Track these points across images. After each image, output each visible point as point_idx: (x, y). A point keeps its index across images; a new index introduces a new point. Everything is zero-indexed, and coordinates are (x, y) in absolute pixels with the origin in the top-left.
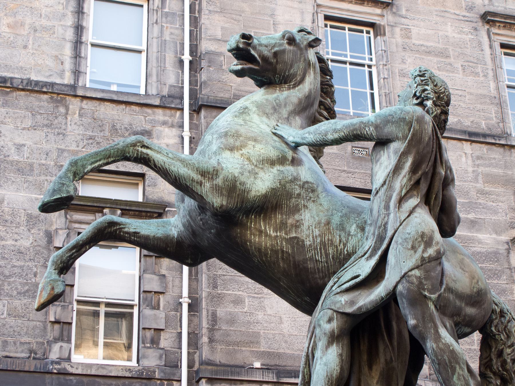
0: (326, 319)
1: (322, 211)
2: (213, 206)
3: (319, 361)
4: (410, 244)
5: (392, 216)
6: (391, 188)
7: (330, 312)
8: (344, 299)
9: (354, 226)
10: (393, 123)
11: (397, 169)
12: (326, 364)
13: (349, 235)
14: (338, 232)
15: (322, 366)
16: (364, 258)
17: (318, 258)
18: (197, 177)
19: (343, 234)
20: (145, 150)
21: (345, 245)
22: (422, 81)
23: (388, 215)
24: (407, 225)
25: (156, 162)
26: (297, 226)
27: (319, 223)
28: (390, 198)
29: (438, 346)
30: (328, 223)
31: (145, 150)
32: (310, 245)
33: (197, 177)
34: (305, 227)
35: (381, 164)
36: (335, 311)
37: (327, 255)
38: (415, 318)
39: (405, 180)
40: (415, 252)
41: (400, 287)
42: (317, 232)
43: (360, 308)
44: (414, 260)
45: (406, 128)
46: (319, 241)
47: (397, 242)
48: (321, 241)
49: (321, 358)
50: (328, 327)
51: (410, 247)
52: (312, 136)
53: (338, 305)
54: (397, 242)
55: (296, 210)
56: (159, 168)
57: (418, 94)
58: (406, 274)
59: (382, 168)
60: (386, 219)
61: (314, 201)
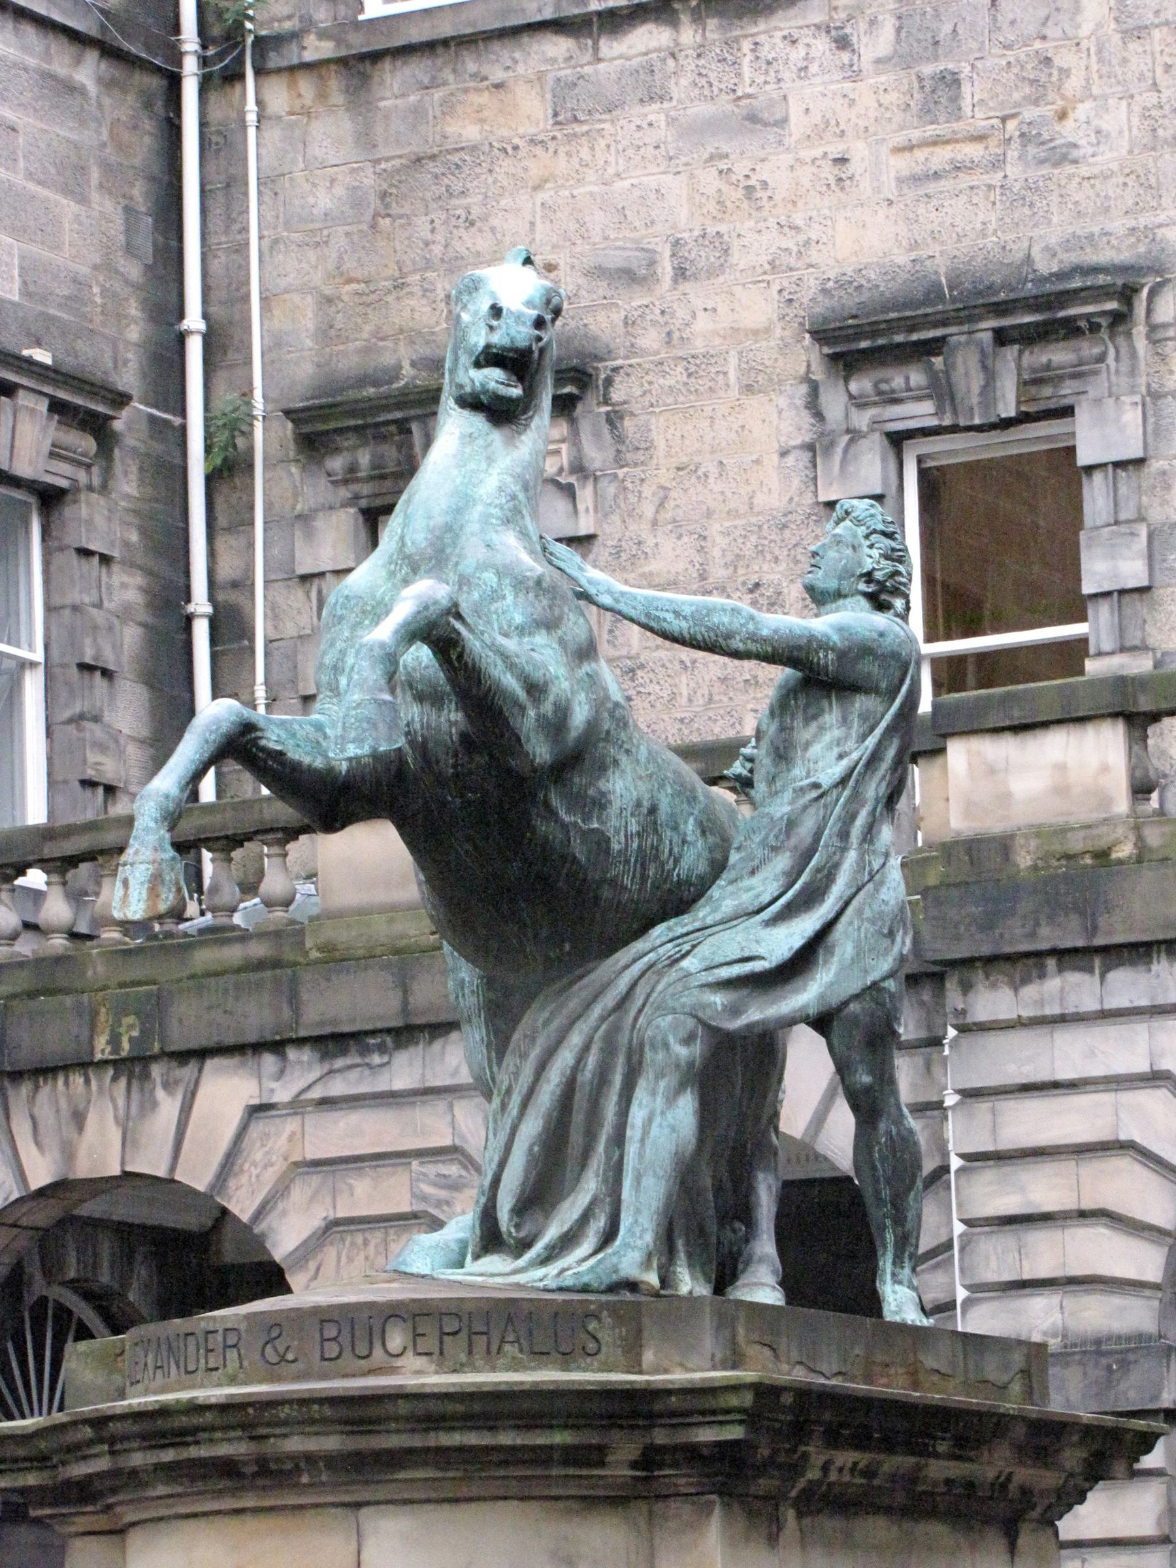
0: (683, 1034)
1: (641, 778)
2: (532, 761)
3: (657, 1120)
4: (888, 923)
5: (852, 855)
6: (856, 796)
7: (691, 1023)
8: (718, 999)
9: (691, 820)
10: (876, 657)
11: (875, 758)
12: (673, 1129)
13: (684, 842)
14: (669, 833)
15: (666, 1131)
16: (759, 918)
17: (627, 882)
18: (521, 694)
19: (676, 839)
20: (458, 625)
21: (677, 861)
22: (893, 550)
23: (844, 850)
24: (882, 883)
25: (467, 651)
26: (600, 803)
27: (639, 804)
28: (853, 817)
29: (898, 1133)
30: (653, 810)
31: (458, 625)
32: (620, 851)
33: (521, 694)
34: (613, 810)
35: (822, 729)
36: (700, 1020)
37: (644, 878)
38: (871, 1072)
39: (884, 784)
40: (893, 941)
41: (853, 1007)
42: (634, 827)
43: (750, 1026)
44: (890, 959)
45: (898, 674)
46: (635, 846)
47: (860, 912)
48: (640, 847)
49: (663, 1113)
50: (682, 1051)
51: (886, 931)
52: (684, 624)
53: (709, 1012)
54: (860, 912)
55: (602, 768)
56: (466, 664)
57: (878, 575)
58: (875, 984)
59: (827, 738)
60: (837, 857)
61: (627, 751)
